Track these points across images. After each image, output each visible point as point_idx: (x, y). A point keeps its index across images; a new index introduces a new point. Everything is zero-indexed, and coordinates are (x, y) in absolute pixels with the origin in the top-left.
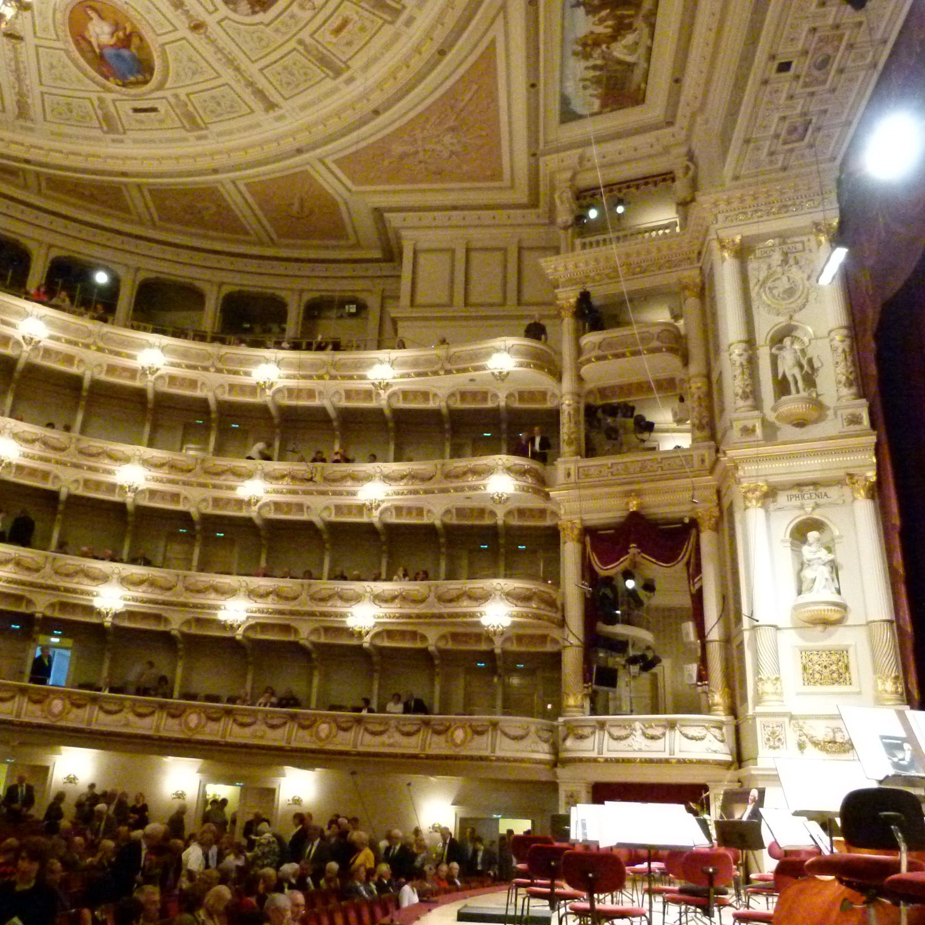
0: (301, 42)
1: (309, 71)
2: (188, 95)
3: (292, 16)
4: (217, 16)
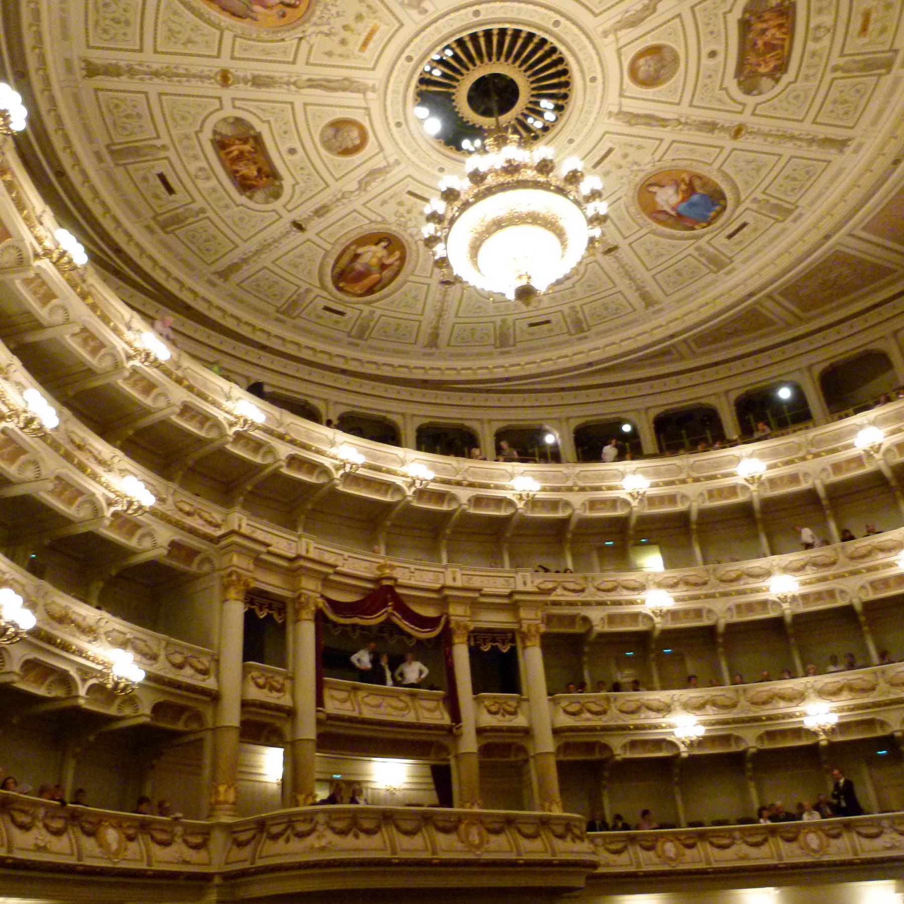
0: (835, 69)
1: (859, 87)
2: (764, 192)
3: (813, 54)
4: (748, 111)
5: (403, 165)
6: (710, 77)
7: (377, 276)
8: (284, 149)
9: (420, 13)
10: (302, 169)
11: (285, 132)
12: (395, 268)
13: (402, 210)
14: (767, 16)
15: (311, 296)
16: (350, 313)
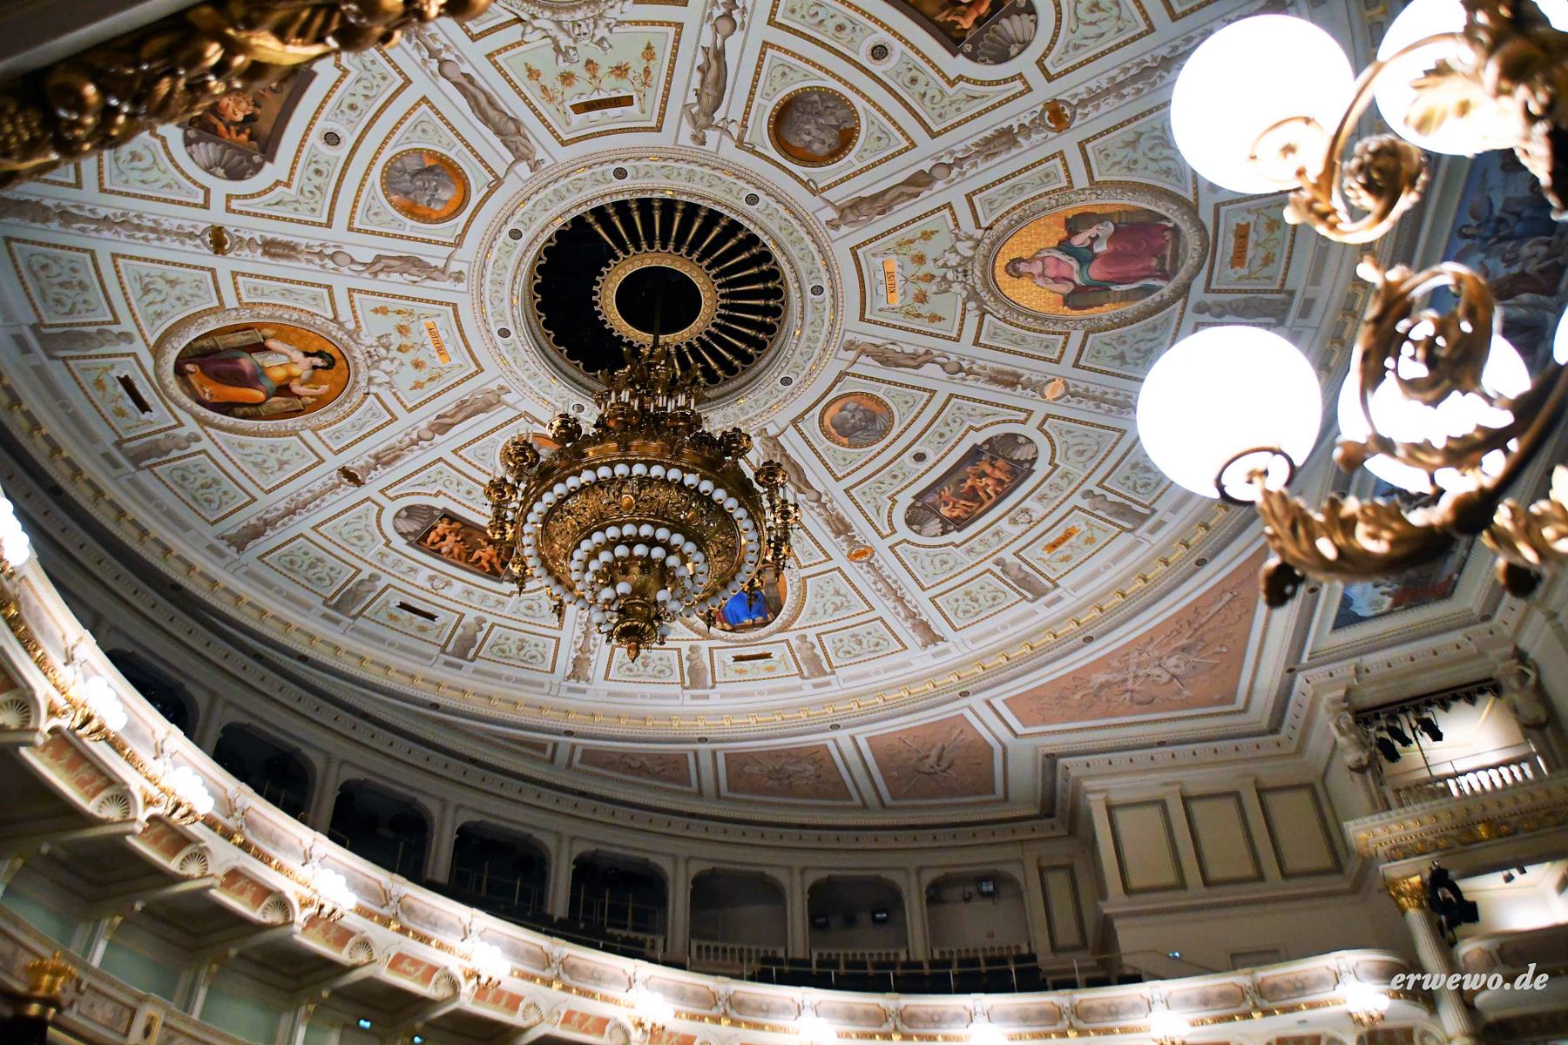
5: (462, 286)
6: (895, 477)
7: (261, 395)
8: (322, 126)
9: (694, 137)
10: (318, 172)
11: (352, 107)
12: (299, 404)
13: (396, 339)
14: (1000, 463)
15: (124, 347)
16: (159, 415)
